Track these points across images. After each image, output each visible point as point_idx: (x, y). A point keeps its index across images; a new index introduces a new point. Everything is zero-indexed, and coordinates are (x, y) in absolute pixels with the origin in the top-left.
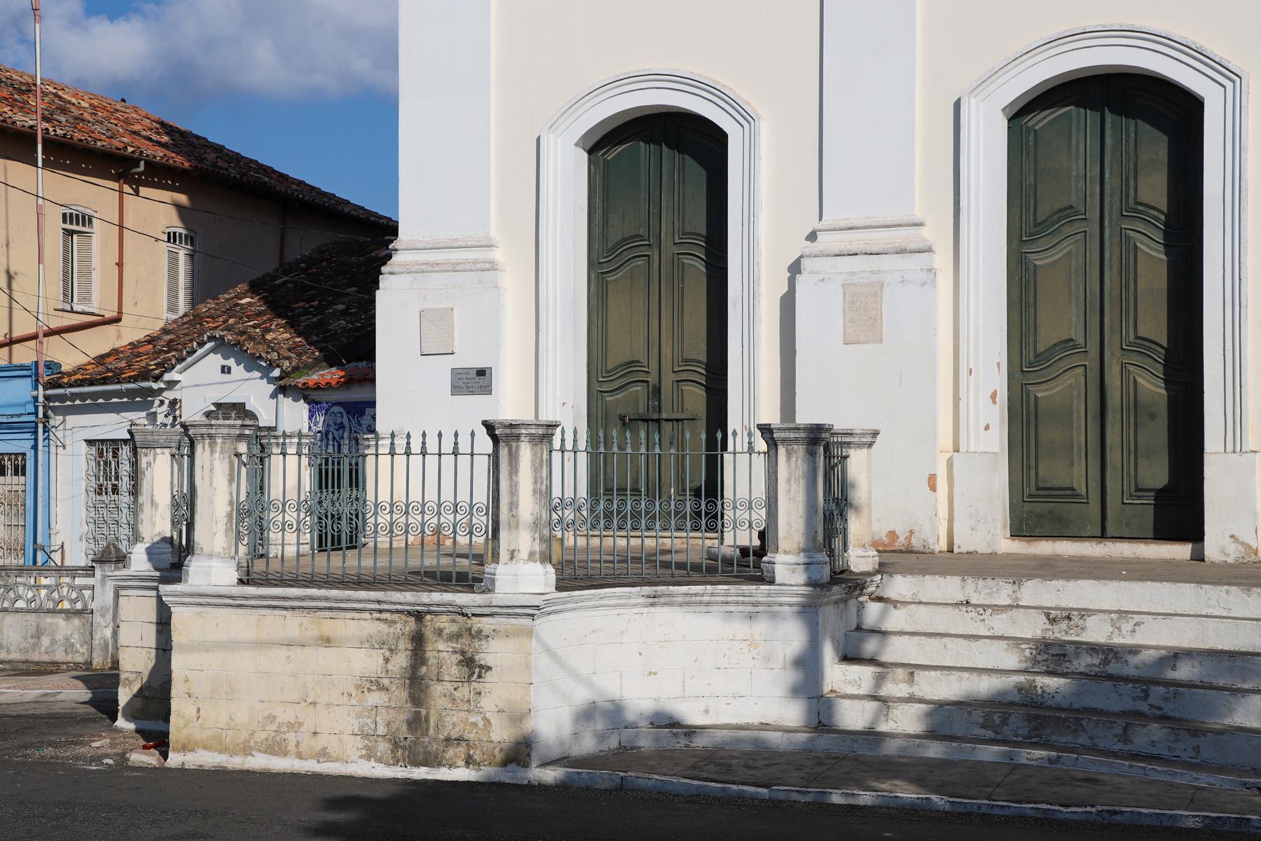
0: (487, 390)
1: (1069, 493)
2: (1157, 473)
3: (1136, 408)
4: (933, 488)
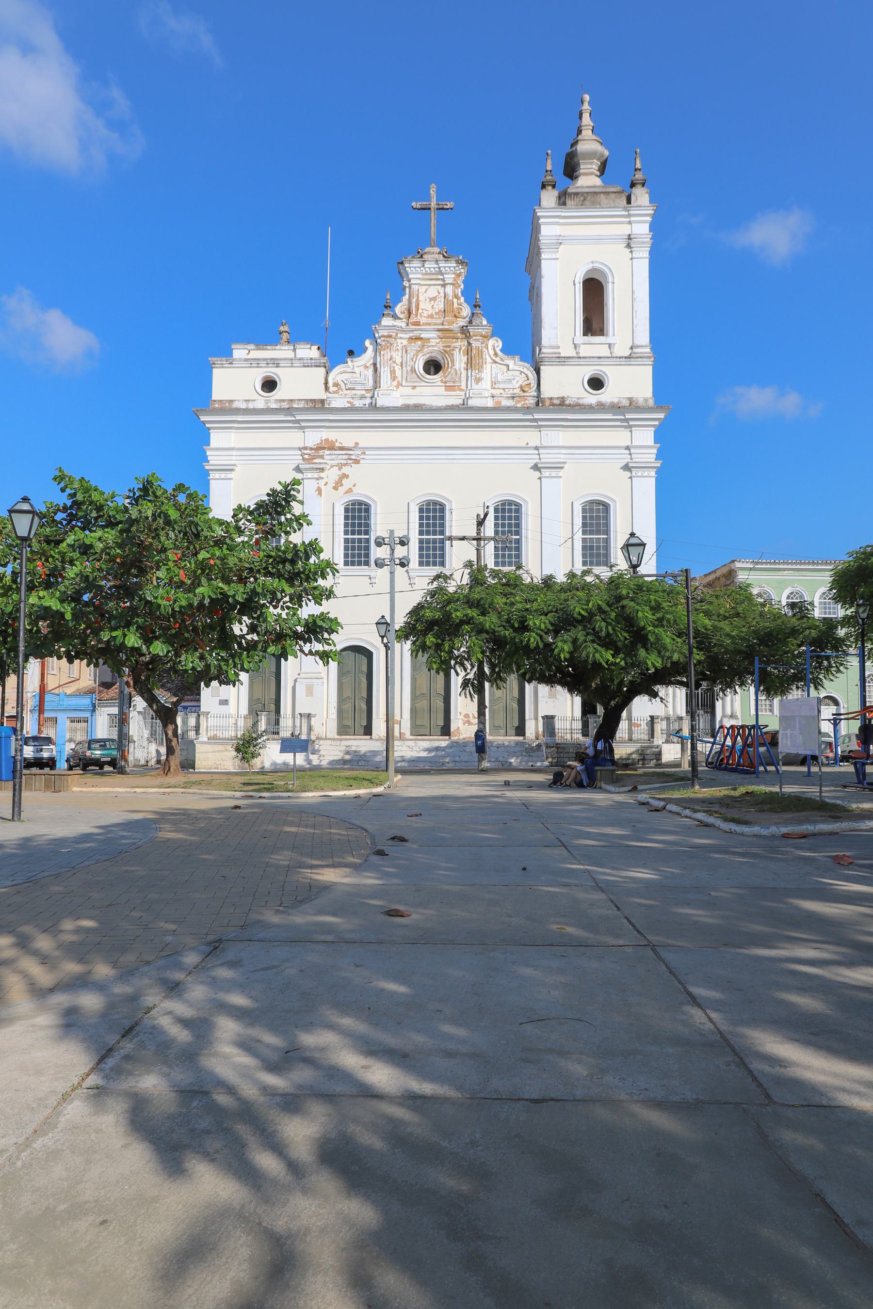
0: (227, 704)
1: (348, 727)
2: (364, 723)
3: (361, 710)
4: (323, 725)
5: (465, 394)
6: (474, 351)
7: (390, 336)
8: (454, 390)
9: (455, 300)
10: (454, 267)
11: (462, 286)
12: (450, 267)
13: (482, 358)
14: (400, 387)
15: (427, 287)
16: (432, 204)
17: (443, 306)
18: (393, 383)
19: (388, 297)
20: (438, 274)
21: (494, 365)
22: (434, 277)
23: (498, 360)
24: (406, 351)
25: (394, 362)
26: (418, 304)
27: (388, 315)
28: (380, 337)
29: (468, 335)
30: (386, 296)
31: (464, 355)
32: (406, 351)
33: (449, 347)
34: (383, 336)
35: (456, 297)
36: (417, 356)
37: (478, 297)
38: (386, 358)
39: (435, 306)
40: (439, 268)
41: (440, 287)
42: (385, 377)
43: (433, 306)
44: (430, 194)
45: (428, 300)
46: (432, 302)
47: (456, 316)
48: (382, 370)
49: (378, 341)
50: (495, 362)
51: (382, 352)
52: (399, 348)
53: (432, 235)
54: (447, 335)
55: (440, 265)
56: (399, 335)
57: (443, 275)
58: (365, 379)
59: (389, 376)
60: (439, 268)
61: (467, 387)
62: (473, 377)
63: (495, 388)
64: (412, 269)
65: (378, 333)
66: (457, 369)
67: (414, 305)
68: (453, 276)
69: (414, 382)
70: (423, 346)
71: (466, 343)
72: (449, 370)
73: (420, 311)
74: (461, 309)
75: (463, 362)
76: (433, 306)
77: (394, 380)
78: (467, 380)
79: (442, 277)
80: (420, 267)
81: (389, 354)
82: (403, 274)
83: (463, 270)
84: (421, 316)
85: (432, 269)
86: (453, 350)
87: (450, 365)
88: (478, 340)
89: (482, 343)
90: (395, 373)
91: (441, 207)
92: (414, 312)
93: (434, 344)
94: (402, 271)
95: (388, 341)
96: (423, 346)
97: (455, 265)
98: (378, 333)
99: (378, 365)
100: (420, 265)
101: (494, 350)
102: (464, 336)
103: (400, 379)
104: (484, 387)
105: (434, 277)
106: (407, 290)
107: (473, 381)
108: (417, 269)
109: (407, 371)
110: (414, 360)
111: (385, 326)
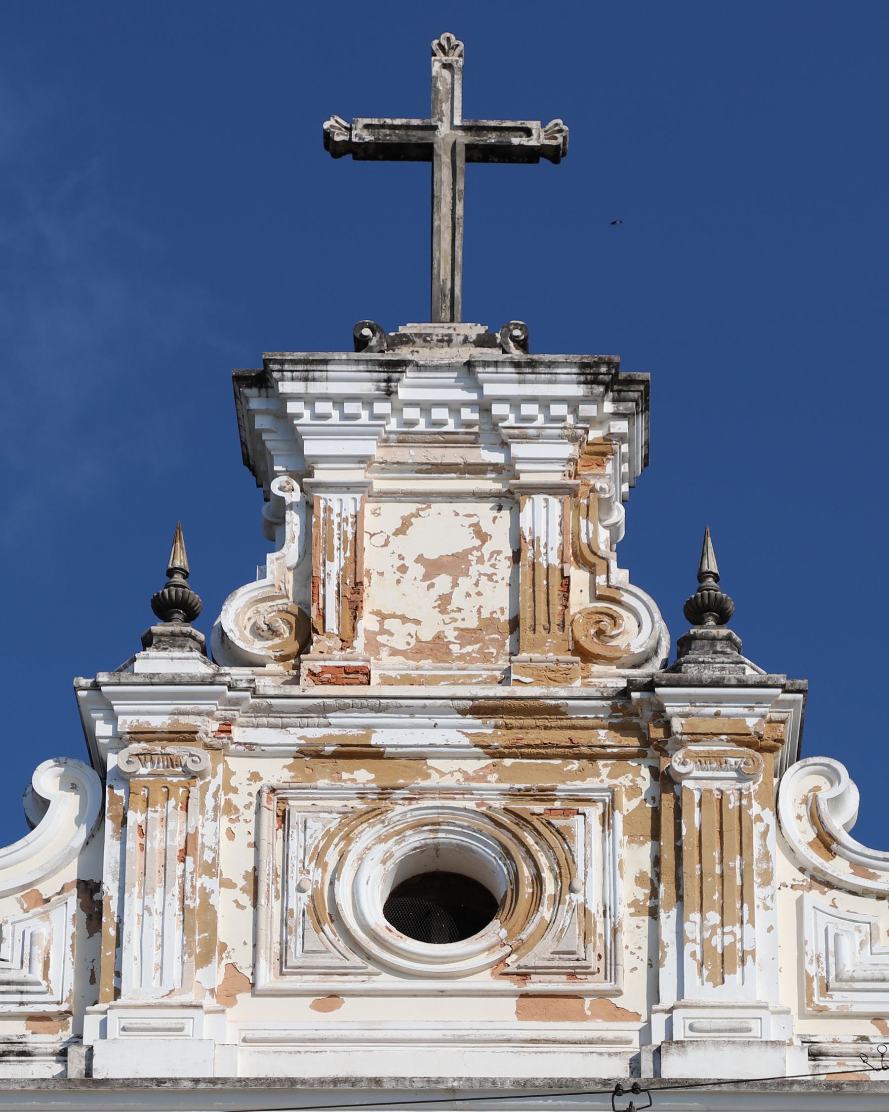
5: (646, 1033)
6: (694, 818)
7: (188, 736)
8: (584, 1018)
9: (579, 577)
10: (573, 404)
11: (618, 514)
12: (545, 403)
13: (743, 848)
14: (244, 998)
15: (409, 508)
16: (444, 129)
17: (506, 603)
18: (200, 975)
19: (180, 560)
20: (474, 441)
21: (815, 897)
22: (452, 455)
23: (839, 869)
24: (283, 818)
25: (211, 869)
26: (358, 585)
27: (175, 640)
28: (120, 741)
29: (657, 733)
30: (167, 552)
31: (633, 838)
32: (283, 818)
33: (543, 795)
34: (137, 735)
35: (581, 561)
36: (348, 838)
37: (711, 564)
38: (155, 842)
39: (457, 600)
40: (484, 407)
41: (484, 511)
42: (151, 941)
43: (444, 602)
44: (429, 81)
45: (418, 570)
46: (443, 582)
47: (578, 650)
48: (133, 906)
49: (112, 761)
50: (829, 885)
51: (134, 818)
52: (239, 800)
53: (443, 270)
54: (534, 737)
55: (489, 390)
56: (238, 734)
57: (504, 445)
58: (26, 961)
59: (175, 936)
60: (484, 407)
61: (654, 995)
62: (688, 948)
63: (821, 1013)
64: (322, 407)
65: (112, 718)
66: (595, 907)
67: (331, 590)
68: (568, 450)
69: (328, 972)
70: (384, 793)
71: (645, 780)
72: (546, 912)
73: (367, 622)
74: (613, 618)
75: (631, 872)
76: (444, 602)
77: (204, 960)
78: (654, 964)
79: (498, 458)
80: (367, 402)
81: (177, 824)
82: (271, 442)
83: (621, 426)
84: (373, 646)
85: (439, 414)
86: (566, 813)
87: (550, 887)
88: (719, 759)
89: (742, 776)
90: (211, 926)
91: (492, 138)
92: (332, 624)
93: (449, 782)
94: (261, 422)
95: (173, 762)
96: (384, 793)
97: (579, 391)
98: (112, 718)
99: (110, 886)
100: (368, 388)
101: (816, 819)
102: (634, 741)
103: (242, 958)
104: (761, 996)
105: (452, 455)
106: (293, 522)
107: (691, 966)
108: (350, 408)
109: (286, 915)
110: (331, 858)
111: (151, 680)
